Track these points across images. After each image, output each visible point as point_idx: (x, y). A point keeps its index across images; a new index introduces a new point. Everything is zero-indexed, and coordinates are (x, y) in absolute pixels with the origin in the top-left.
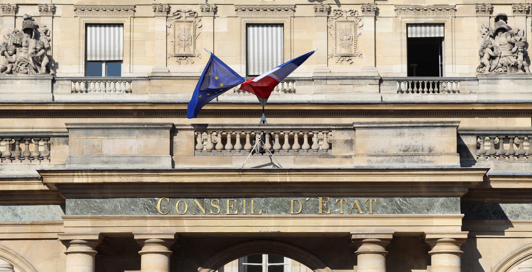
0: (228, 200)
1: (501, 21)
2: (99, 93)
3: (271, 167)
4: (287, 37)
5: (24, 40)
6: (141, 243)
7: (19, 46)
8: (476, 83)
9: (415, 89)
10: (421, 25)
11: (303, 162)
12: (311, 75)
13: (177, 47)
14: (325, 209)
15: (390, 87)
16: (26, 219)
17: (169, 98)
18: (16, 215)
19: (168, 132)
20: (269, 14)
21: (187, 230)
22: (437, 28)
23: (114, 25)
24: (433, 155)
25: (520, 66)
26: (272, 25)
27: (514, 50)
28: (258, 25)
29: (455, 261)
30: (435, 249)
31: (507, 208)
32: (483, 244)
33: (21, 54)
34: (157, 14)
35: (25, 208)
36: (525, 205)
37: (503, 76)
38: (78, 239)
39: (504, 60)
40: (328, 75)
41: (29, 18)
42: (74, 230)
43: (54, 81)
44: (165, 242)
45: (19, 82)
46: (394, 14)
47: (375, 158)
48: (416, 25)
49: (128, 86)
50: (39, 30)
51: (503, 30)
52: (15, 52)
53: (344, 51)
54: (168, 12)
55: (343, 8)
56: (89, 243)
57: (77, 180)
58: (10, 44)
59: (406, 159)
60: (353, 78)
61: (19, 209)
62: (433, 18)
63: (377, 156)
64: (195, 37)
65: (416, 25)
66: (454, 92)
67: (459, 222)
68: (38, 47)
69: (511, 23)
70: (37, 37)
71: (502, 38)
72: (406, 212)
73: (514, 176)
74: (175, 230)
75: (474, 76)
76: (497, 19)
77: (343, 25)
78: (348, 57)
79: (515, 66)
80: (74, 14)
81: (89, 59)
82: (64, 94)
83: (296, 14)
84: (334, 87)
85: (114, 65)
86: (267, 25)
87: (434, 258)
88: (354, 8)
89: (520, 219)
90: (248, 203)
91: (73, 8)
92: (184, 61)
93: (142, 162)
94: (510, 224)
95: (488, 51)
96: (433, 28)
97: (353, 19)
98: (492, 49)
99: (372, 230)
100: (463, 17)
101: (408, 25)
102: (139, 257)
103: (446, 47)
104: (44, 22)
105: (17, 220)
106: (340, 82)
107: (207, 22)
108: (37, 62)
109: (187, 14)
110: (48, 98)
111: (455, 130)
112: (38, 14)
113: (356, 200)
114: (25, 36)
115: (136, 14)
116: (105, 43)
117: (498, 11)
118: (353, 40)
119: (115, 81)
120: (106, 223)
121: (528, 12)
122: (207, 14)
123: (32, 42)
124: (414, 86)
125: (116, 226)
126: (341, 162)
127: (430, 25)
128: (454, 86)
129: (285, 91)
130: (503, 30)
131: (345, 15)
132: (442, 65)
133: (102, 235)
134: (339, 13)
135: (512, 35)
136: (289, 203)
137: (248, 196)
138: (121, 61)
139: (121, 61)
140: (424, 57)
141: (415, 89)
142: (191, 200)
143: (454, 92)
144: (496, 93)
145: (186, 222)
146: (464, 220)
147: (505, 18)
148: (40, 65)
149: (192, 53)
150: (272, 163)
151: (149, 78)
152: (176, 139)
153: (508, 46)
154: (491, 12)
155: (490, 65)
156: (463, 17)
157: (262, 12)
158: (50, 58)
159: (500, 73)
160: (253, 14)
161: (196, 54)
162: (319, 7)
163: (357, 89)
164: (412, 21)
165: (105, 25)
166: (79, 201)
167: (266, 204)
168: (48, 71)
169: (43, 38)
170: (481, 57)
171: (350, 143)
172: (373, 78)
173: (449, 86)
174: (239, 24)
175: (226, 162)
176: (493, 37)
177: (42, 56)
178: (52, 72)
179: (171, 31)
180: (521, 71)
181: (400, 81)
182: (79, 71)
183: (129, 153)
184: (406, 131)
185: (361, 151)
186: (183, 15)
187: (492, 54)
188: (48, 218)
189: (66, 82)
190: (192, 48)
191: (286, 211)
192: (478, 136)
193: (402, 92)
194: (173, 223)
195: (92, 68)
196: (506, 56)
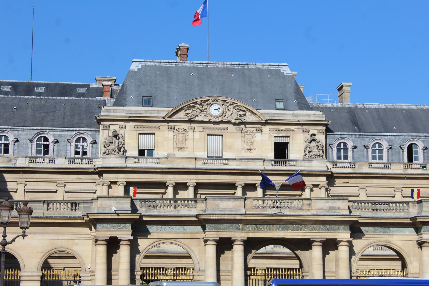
0: (266, 226)
1: (313, 136)
2: (144, 163)
3: (280, 214)
4: (224, 141)
5: (114, 140)
6: (235, 241)
7: (112, 143)
8: (303, 162)
9: (278, 164)
10: (280, 137)
11: (293, 212)
12: (234, 157)
13: (178, 144)
14: (301, 229)
16: (188, 231)
17: (175, 166)
18: (185, 229)
19: (244, 200)
20: (217, 130)
21: (251, 236)
22: (286, 138)
23: (151, 134)
24: (340, 210)
25: (321, 155)
26: (218, 135)
27: (319, 149)
28: (212, 135)
29: (347, 249)
30: (340, 244)
31: (363, 229)
32: (355, 242)
33: (112, 146)
34: (170, 130)
35: (188, 227)
36: (370, 228)
37: (314, 160)
38: (211, 239)
39: (314, 153)
40: (241, 157)
41: (116, 131)
42: (209, 236)
43: (126, 158)
44: (243, 241)
45: (112, 158)
46: (269, 132)
47: (319, 211)
48: (278, 137)
49: (158, 161)
50: (119, 136)
51: (314, 140)
52: (110, 146)
53: (248, 147)
54: (174, 129)
55: (247, 129)
56: (215, 241)
57: (212, 217)
58: (107, 141)
59: (330, 211)
60: (253, 159)
61: (186, 227)
63: (320, 210)
64: (186, 140)
65: (278, 137)
66: (294, 166)
67: (349, 235)
68: (120, 144)
69: (317, 137)
70: (119, 139)
71: (314, 144)
72: (330, 231)
73: (367, 218)
74: (247, 237)
76: (311, 135)
77: (248, 136)
78: (250, 150)
79: (319, 155)
80: (134, 129)
81: (140, 148)
82: (131, 164)
83: (228, 131)
85: (151, 151)
86: (216, 135)
87: (339, 247)
88: (252, 129)
89: (368, 233)
90: (273, 226)
91: (133, 126)
92: (180, 150)
93: (234, 211)
94: (364, 235)
95: (308, 149)
96: (285, 138)
97: (252, 134)
98: (310, 148)
99: (318, 237)
101: (275, 137)
102: (233, 246)
103: (290, 146)
104: (121, 132)
105: (185, 231)
106: (247, 160)
107: (190, 134)
108: (119, 149)
109: (182, 130)
110: (124, 165)
111: (347, 201)
112: (118, 129)
113: (312, 226)
114: (114, 138)
115: (160, 130)
116: (146, 142)
117: (312, 132)
118: (251, 143)
119: (152, 158)
120: (221, 233)
121: (324, 133)
122: (191, 130)
123: (117, 141)
124: (277, 163)
125: (225, 234)
126: (306, 212)
127: (284, 137)
128: (294, 163)
129: (224, 164)
130: (314, 140)
131: (248, 132)
132: (288, 154)
133: (220, 238)
134: (246, 131)
135: (318, 142)
136: (288, 227)
137: (273, 224)
138: (154, 150)
139: (154, 150)
140: (281, 150)
141: (278, 164)
142: (252, 225)
143: (294, 166)
144: (311, 167)
145: (250, 234)
146: (351, 234)
147: (315, 135)
148: (120, 151)
149: (184, 146)
150: (281, 212)
151: (167, 158)
152: (246, 202)
153: (316, 147)
154: (309, 132)
155: (308, 154)
157: (217, 130)
158: (124, 148)
159: (313, 158)
160: (210, 131)
161: (186, 147)
162: (238, 128)
163: (254, 164)
164: (277, 135)
165: (147, 134)
166: (211, 225)
167: (280, 227)
168: (123, 154)
169: (121, 140)
170: (305, 151)
171: (309, 205)
172: (261, 159)
173: (292, 163)
174: (204, 134)
175: (264, 211)
176: (310, 143)
177: (121, 147)
178: (125, 154)
179: (175, 137)
180: (321, 158)
181: (272, 161)
182: (136, 154)
183: (229, 208)
184: (330, 201)
185: (314, 208)
186: (180, 130)
187: (310, 150)
188: (196, 231)
189: (132, 159)
190: (184, 144)
191: (287, 230)
192: (353, 202)
193: (273, 165)
194: (246, 234)
195: (142, 153)
196: (315, 151)
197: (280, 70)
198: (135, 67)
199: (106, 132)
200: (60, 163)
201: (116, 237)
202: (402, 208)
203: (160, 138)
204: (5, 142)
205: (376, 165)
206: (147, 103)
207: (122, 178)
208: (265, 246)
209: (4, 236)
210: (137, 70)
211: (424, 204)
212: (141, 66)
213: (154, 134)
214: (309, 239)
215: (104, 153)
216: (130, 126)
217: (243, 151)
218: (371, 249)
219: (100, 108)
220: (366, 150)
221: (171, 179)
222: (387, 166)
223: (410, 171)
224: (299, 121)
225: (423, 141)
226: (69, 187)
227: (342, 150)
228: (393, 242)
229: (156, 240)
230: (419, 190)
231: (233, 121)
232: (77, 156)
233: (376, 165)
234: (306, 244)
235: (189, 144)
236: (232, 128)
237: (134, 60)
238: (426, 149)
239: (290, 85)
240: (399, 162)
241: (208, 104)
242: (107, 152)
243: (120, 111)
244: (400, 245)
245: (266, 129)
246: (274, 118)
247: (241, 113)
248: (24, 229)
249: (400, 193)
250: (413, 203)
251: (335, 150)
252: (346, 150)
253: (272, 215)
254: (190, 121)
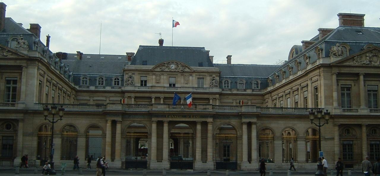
2: (143, 89)
4: (176, 79)
12: (180, 86)
30: (209, 123)
45: (129, 87)
53: (186, 82)
56: (156, 122)
71: (214, 81)
75: (209, 87)
79: (216, 86)
82: (137, 89)
99: (199, 121)
107: (162, 77)
125: (160, 119)
147: (214, 77)
151: (152, 87)
171: (196, 107)
191: (186, 117)
199: (127, 76)
200: (108, 88)
201: (115, 120)
202: (234, 108)
203: (149, 78)
204: (86, 80)
205: (241, 90)
206: (145, 63)
207: (133, 95)
208: (180, 123)
209: (53, 119)
211: (243, 107)
212: (143, 48)
213: (147, 77)
214: (195, 121)
215: (126, 84)
216: (136, 73)
217: (184, 84)
218: (222, 125)
219: (125, 66)
220: (236, 84)
221: (153, 95)
222: (245, 90)
223: (254, 93)
224: (208, 71)
225: (260, 80)
226: (111, 99)
227: (226, 84)
228: (232, 123)
229: (132, 121)
230: (242, 101)
231: (180, 71)
232: (115, 86)
233: (241, 90)
234: (194, 124)
235: (162, 81)
236: (179, 75)
238: (262, 83)
240: (250, 89)
241: (170, 64)
242: (127, 84)
243: (133, 67)
244: (234, 124)
245: (194, 75)
246: (197, 70)
247: (184, 68)
248: (61, 117)
249: (250, 102)
250: (240, 106)
251: (223, 83)
252: (228, 83)
253: (180, 111)
254: (162, 71)
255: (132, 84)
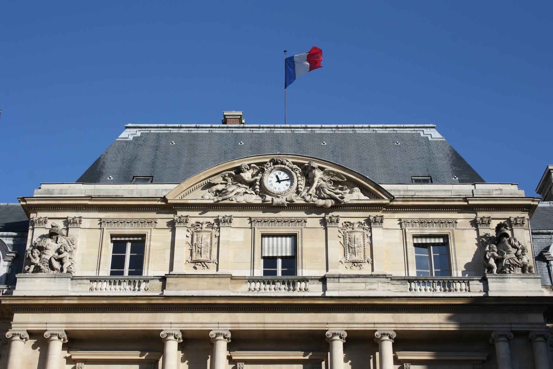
13: (194, 254)
15: (401, 286)
62: (437, 229)
84: (346, 284)
100: (465, 229)
107: (225, 232)
144: (506, 291)
156: (465, 229)
164: (418, 232)
197: (419, 134)
198: (128, 135)
210: (131, 138)
237: (130, 125)
239: (441, 155)
255: (58, 266)
